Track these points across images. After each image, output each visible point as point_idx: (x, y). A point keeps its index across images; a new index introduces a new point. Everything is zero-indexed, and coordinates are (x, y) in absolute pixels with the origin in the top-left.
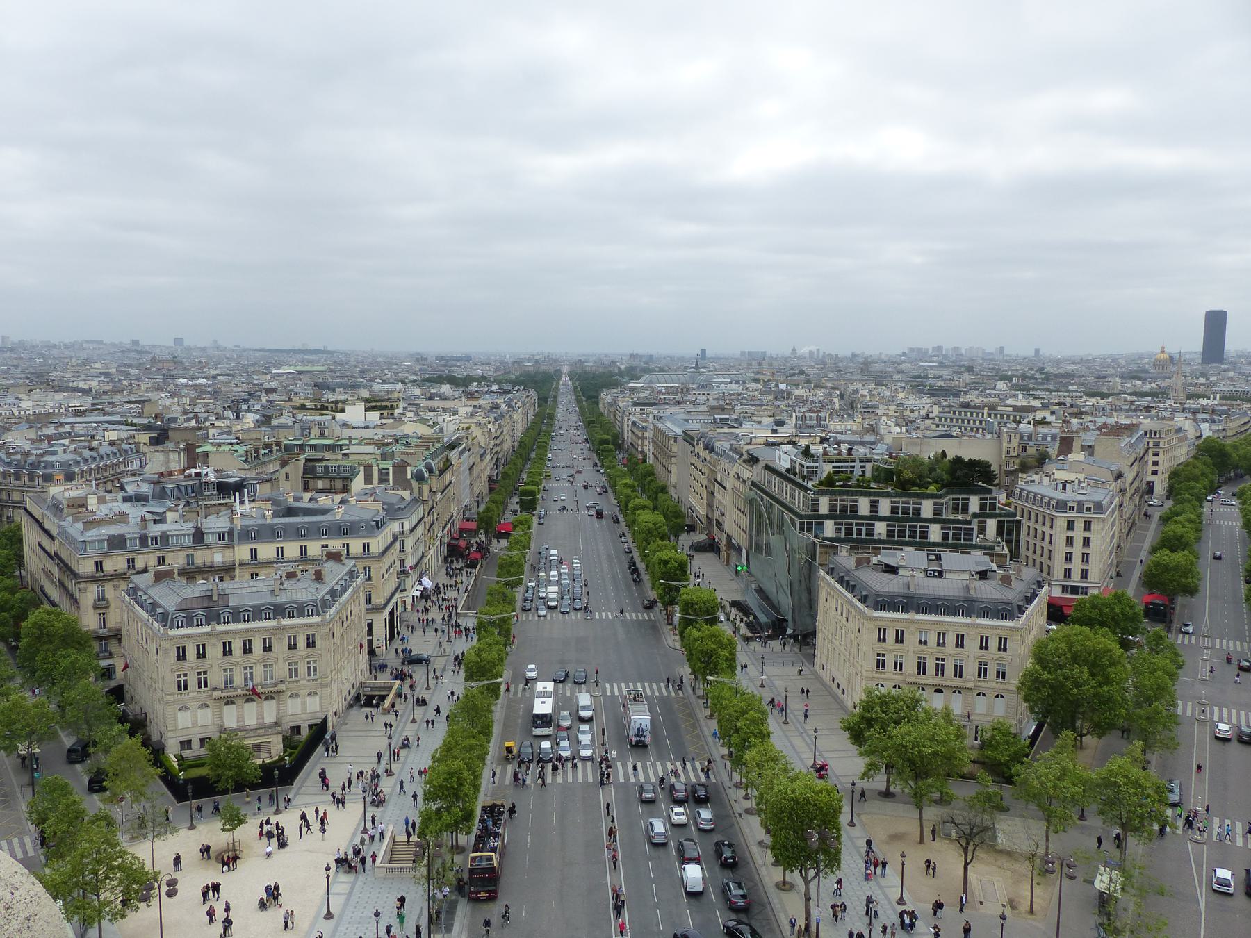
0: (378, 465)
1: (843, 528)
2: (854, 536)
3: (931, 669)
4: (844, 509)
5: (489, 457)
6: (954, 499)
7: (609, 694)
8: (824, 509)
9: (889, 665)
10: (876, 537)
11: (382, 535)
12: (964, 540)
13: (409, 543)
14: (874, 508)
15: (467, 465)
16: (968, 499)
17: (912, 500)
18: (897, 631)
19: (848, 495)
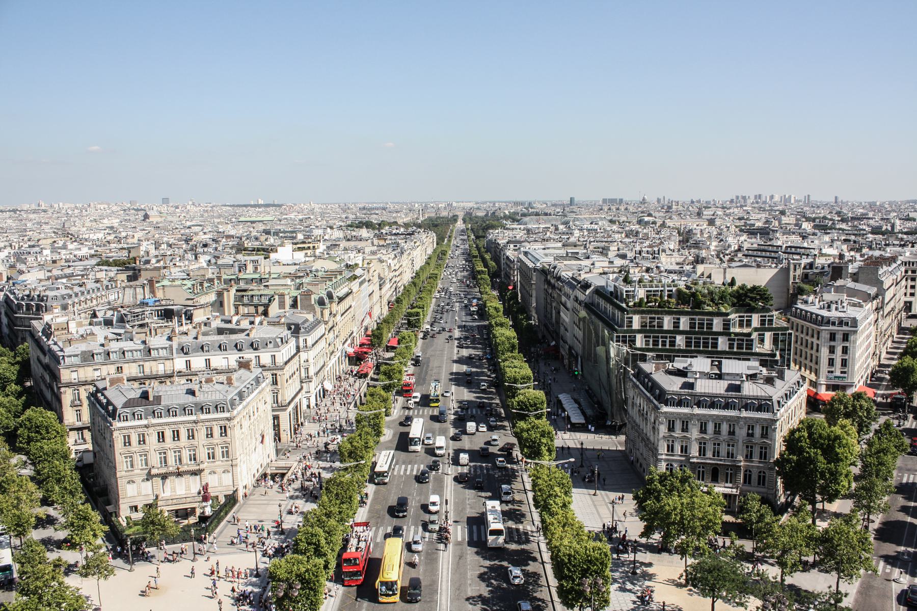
1: (651, 340)
2: (660, 347)
6: (740, 317)
8: (636, 325)
10: (676, 348)
11: (286, 349)
12: (746, 349)
14: (676, 324)
16: (751, 317)
17: (706, 317)
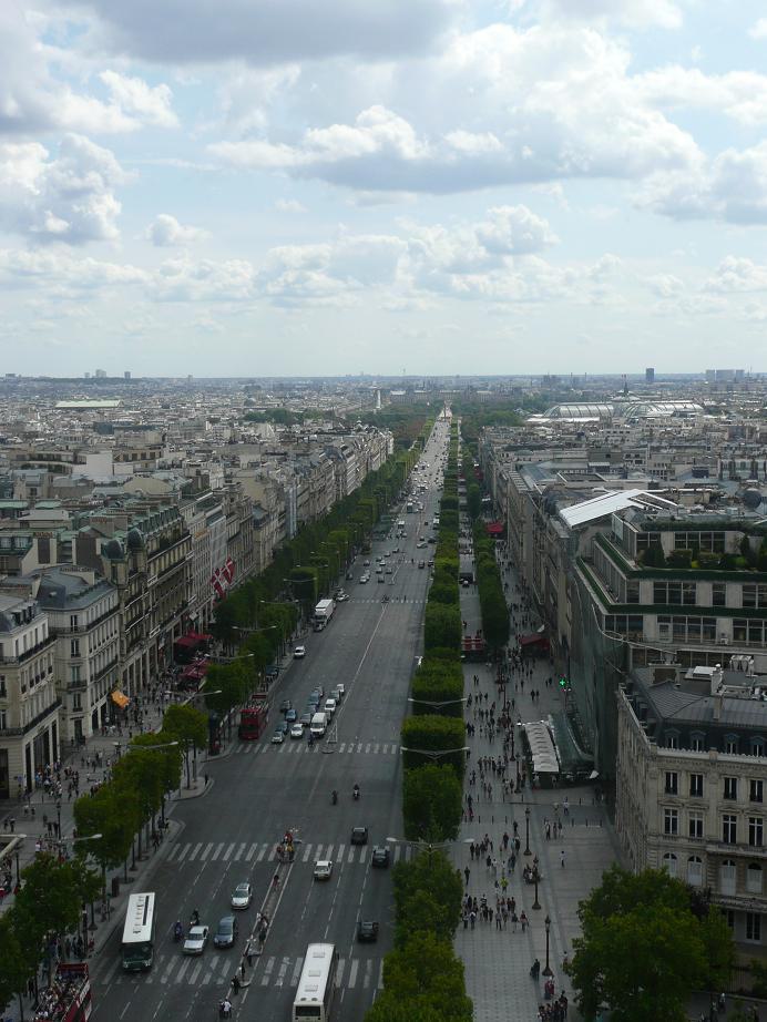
0: (58, 536)
1: (671, 625)
3: (743, 835)
4: (675, 596)
5: (275, 523)
7: (305, 859)
9: (683, 827)
11: (27, 632)
13: (85, 644)
14: (719, 599)
18: (693, 777)
19: (664, 578)
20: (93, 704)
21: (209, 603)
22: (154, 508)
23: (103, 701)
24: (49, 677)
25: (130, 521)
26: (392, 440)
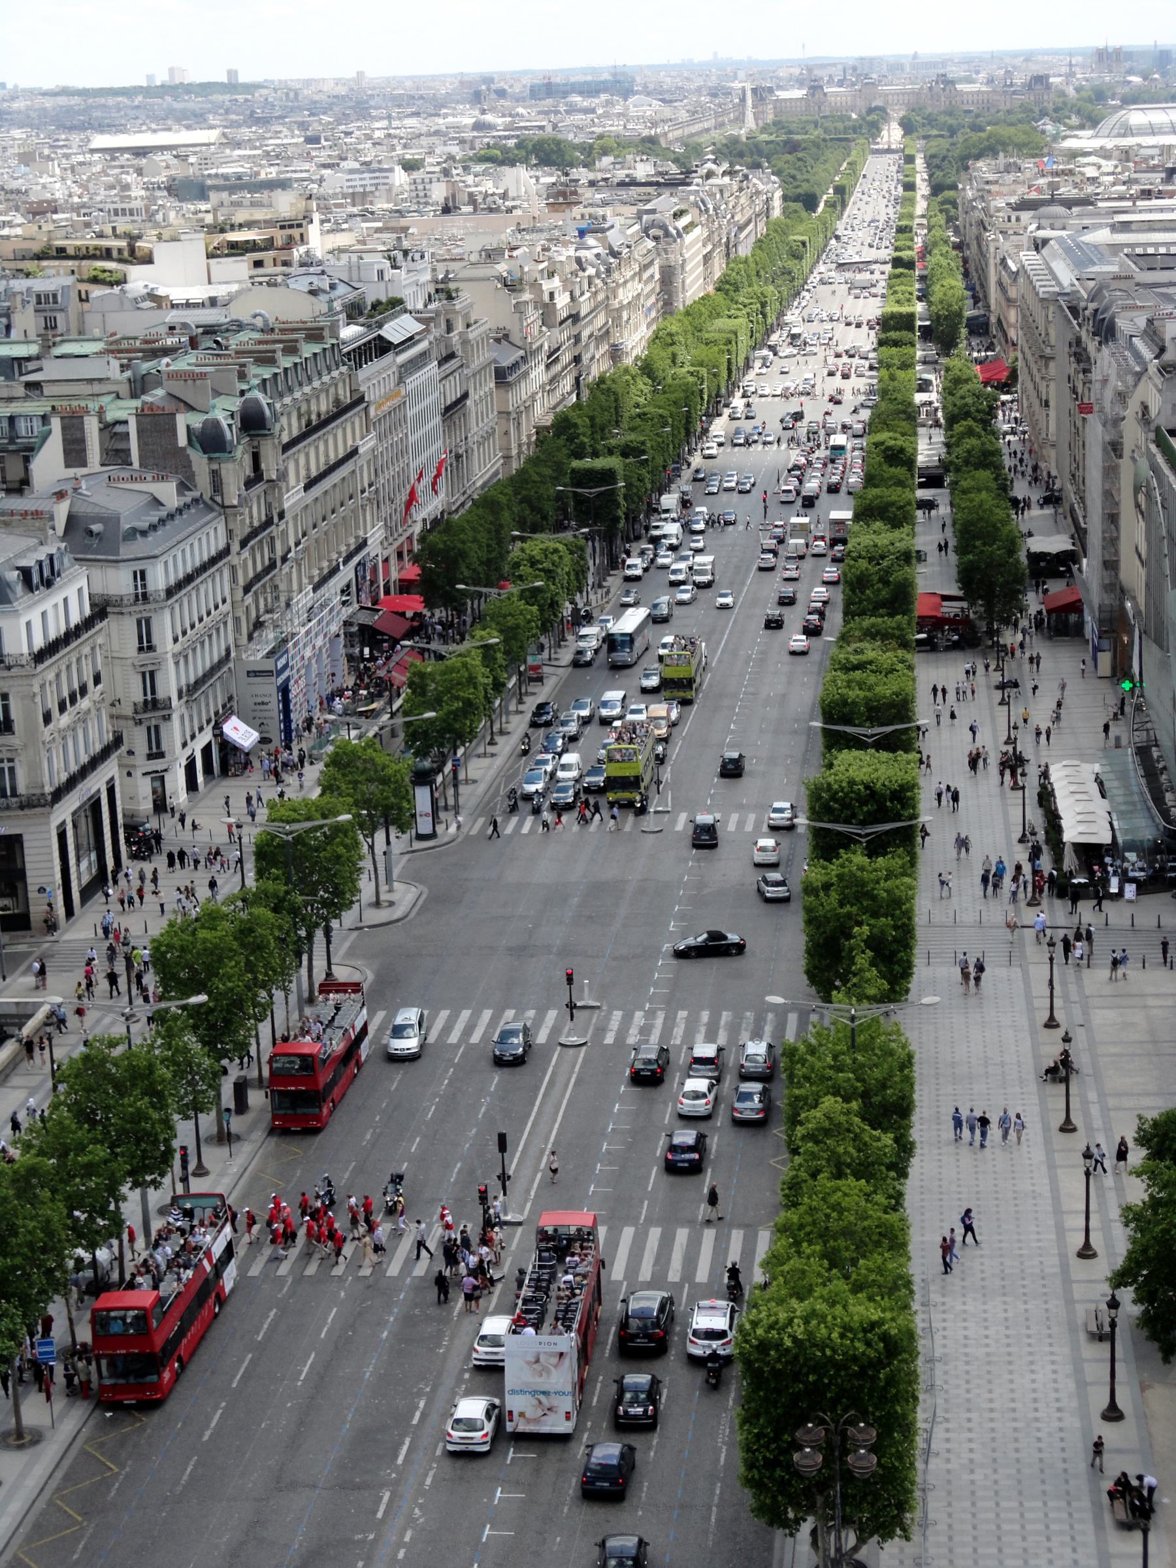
0: (101, 412)
11: (47, 605)
15: (434, 400)
20: (185, 745)
21: (410, 538)
22: (291, 349)
23: (206, 737)
24: (94, 692)
25: (242, 376)
26: (778, 194)
